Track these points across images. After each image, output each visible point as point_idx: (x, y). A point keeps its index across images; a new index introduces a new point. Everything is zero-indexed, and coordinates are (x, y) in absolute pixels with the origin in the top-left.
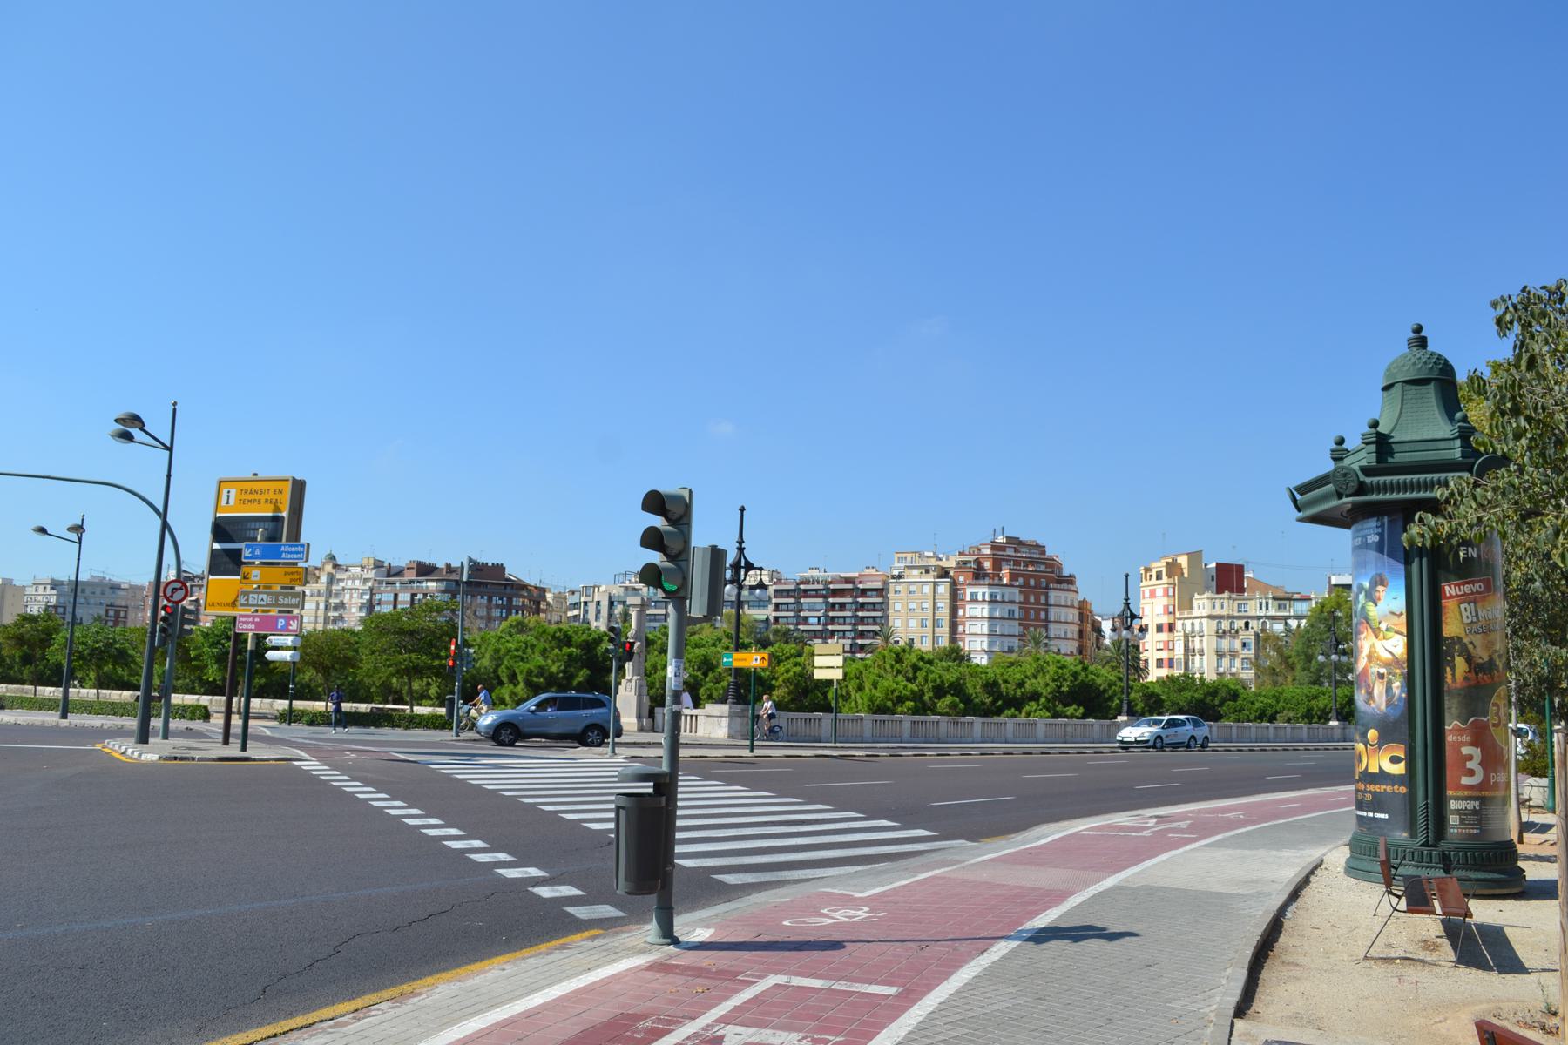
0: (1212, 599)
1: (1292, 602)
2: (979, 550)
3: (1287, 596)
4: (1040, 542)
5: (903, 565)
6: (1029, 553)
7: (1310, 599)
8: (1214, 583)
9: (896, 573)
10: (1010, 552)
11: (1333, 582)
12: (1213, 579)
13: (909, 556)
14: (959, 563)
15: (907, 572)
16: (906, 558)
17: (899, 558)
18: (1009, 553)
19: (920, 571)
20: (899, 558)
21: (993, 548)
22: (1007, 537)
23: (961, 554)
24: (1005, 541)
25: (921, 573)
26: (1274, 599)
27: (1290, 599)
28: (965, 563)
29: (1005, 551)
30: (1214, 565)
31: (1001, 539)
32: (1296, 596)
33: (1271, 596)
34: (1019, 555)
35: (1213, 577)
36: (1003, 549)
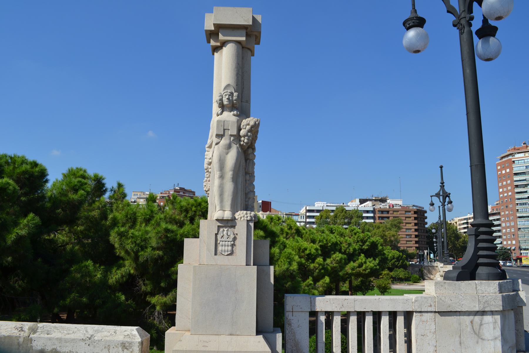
0: (263, 214)
1: (292, 216)
2: (169, 192)
3: (291, 214)
4: (193, 190)
5: (136, 197)
6: (189, 194)
7: (299, 215)
8: (261, 208)
9: (133, 200)
10: (181, 193)
11: (308, 209)
12: (260, 207)
13: (139, 194)
14: (160, 197)
15: (138, 200)
16: (137, 194)
17: (134, 194)
18: (180, 194)
19: (144, 200)
20: (134, 194)
21: (175, 191)
22: (180, 188)
23: (161, 193)
24: (179, 189)
25: (144, 201)
26: (286, 215)
27: (292, 215)
28: (163, 197)
29: (180, 193)
30: (261, 201)
31: (177, 188)
32: (293, 214)
33: (285, 214)
34: (185, 195)
35: (260, 206)
36: (179, 192)
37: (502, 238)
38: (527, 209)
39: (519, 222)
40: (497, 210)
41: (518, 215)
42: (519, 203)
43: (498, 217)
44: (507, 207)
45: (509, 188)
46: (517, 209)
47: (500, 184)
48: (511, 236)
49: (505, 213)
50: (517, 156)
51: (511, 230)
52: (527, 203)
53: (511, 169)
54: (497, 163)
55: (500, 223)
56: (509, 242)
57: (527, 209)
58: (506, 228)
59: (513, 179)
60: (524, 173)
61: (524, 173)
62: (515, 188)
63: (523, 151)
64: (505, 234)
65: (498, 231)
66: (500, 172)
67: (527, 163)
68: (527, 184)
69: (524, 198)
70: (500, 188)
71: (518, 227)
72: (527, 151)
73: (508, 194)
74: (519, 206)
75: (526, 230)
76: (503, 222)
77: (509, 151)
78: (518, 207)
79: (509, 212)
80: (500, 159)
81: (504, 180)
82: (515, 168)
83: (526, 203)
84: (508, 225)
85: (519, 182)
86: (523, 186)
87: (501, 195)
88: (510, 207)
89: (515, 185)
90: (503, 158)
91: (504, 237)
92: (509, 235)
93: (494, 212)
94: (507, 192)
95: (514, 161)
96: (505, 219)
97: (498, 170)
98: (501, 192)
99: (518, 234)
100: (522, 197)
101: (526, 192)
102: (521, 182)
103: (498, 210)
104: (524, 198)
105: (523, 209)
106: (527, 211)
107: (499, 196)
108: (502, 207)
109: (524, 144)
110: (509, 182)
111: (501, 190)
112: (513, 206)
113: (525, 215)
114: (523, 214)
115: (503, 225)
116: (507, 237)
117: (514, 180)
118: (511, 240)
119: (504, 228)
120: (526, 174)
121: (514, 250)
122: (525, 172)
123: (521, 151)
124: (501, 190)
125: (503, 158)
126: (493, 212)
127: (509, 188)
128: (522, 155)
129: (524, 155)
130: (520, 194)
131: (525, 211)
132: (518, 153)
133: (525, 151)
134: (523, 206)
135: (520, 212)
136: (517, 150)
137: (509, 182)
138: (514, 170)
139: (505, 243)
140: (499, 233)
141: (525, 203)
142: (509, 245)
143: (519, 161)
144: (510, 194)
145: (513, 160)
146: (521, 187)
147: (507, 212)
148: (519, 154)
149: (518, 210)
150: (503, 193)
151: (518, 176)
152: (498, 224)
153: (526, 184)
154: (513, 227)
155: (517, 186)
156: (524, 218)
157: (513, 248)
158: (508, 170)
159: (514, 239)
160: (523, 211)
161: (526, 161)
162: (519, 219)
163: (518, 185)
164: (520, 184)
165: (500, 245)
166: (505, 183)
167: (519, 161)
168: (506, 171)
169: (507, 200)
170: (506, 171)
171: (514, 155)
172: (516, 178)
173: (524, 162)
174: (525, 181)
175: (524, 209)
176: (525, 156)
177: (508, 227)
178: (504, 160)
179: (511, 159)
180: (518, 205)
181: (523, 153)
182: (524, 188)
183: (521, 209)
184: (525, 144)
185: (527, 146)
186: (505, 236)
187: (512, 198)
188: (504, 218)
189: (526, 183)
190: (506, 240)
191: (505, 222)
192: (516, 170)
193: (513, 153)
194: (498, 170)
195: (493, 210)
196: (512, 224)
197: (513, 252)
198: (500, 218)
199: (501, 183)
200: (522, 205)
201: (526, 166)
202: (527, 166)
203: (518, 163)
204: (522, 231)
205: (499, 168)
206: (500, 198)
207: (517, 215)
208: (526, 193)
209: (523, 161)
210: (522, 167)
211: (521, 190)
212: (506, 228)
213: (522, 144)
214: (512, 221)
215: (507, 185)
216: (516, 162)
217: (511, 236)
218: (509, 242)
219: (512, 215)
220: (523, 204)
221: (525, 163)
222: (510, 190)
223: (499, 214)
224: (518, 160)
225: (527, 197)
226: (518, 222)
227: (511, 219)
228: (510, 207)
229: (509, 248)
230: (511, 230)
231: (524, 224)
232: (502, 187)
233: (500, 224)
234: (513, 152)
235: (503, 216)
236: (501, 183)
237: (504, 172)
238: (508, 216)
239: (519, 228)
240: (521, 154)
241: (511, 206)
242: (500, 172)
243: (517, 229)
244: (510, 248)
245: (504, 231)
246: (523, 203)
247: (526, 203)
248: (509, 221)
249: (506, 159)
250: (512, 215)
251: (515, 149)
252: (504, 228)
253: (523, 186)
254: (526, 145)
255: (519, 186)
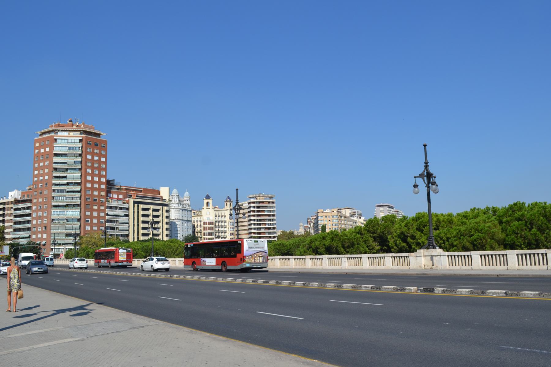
37: (30, 231)
38: (64, 197)
39: (53, 211)
40: (28, 196)
41: (54, 203)
42: (56, 190)
43: (29, 205)
44: (41, 193)
45: (47, 171)
46: (53, 196)
47: (36, 165)
48: (42, 229)
49: (38, 200)
50: (60, 133)
51: (42, 221)
52: (65, 190)
53: (52, 148)
54: (35, 139)
55: (31, 213)
56: (39, 236)
57: (64, 197)
58: (37, 218)
59: (53, 160)
60: (65, 155)
61: (65, 155)
62: (53, 171)
63: (68, 129)
64: (36, 226)
65: (27, 222)
66: (38, 151)
67: (71, 143)
68: (68, 168)
69: (62, 185)
70: (35, 169)
71: (52, 218)
72: (72, 129)
73: (44, 178)
74: (55, 193)
75: (60, 221)
76: (34, 211)
77: (52, 126)
78: (54, 194)
79: (43, 200)
80: (40, 135)
81: (42, 161)
82: (56, 147)
83: (64, 190)
84: (40, 214)
85: (59, 165)
86: (63, 170)
87: (36, 179)
88: (45, 193)
89: (54, 168)
90: (43, 134)
91: (34, 230)
92: (40, 227)
93: (25, 198)
94: (44, 175)
95: (56, 140)
96: (37, 207)
97: (36, 148)
98: (36, 175)
99: (51, 226)
100: (60, 183)
101: (65, 177)
102: (61, 165)
103: (30, 196)
104: (62, 185)
105: (59, 197)
106: (64, 200)
107: (34, 179)
108: (35, 193)
109: (70, 121)
110: (47, 163)
111: (36, 172)
112: (48, 192)
113: (61, 204)
114: (59, 203)
115: (34, 215)
116: (37, 229)
117: (54, 161)
118: (42, 233)
119: (34, 218)
120: (67, 157)
121: (44, 245)
122: (66, 154)
123: (65, 129)
124: (36, 172)
125: (43, 134)
126: (23, 199)
127: (47, 171)
128: (66, 134)
129: (69, 134)
130: (59, 179)
131: (61, 200)
132: (62, 131)
133: (70, 129)
134: (60, 193)
135: (56, 200)
136: (61, 127)
137: (47, 163)
138: (55, 150)
139: (34, 236)
140: (28, 225)
141: (63, 190)
142: (39, 239)
143: (63, 141)
144: (47, 177)
145: (55, 138)
146: (60, 171)
147: (40, 200)
148: (63, 132)
149: (53, 197)
150: (38, 176)
151: (59, 157)
152: (28, 213)
153: (66, 168)
154: (46, 217)
155: (56, 169)
156: (60, 208)
157: (43, 242)
158: (48, 149)
159: (45, 232)
160: (59, 199)
161: (70, 141)
162: (53, 208)
163: (57, 168)
164: (60, 167)
165: (28, 239)
166: (42, 164)
167: (62, 140)
168: (45, 150)
169: (42, 184)
170: (45, 150)
171: (57, 132)
172: (56, 160)
173: (68, 142)
174: (66, 165)
175: (60, 197)
176: (69, 135)
177: (40, 218)
178: (44, 136)
179: (53, 136)
180: (54, 192)
181: (68, 132)
182: (63, 173)
183: (57, 197)
184: (72, 122)
185: (73, 125)
186: (35, 228)
187: (48, 183)
188: (36, 207)
189: (67, 167)
190: (36, 233)
191: (37, 211)
192: (57, 150)
193: (56, 130)
194: (36, 148)
195: (24, 196)
196: (45, 214)
197: (43, 248)
198: (31, 207)
199: (37, 164)
200: (59, 192)
201: (69, 147)
202: (71, 147)
203: (61, 142)
204: (55, 223)
205: (37, 145)
206: (35, 182)
207: (52, 203)
208: (65, 179)
209: (66, 141)
210: (64, 148)
211: (60, 174)
212: (37, 218)
213: (68, 122)
214: (45, 210)
215: (44, 167)
216: (58, 140)
217: (42, 229)
218: (39, 236)
219: (45, 203)
220: (61, 191)
221: (69, 143)
222: (47, 173)
223: (30, 201)
224: (61, 139)
225: (66, 183)
226: (52, 212)
227: (45, 208)
228: (45, 193)
229: (38, 242)
230: (42, 221)
231: (59, 215)
232: (38, 169)
233: (31, 214)
234: (56, 129)
235: (35, 204)
236: (37, 164)
237: (42, 151)
238: (41, 204)
239: (52, 219)
240: (66, 132)
241: (46, 192)
242: (38, 151)
243: (50, 221)
244: (40, 243)
245: (34, 222)
246: (61, 190)
247: (63, 190)
248: (42, 210)
249: (47, 135)
250: (45, 203)
251: (59, 125)
252: (34, 218)
253: (63, 170)
254: (72, 123)
255: (58, 170)
